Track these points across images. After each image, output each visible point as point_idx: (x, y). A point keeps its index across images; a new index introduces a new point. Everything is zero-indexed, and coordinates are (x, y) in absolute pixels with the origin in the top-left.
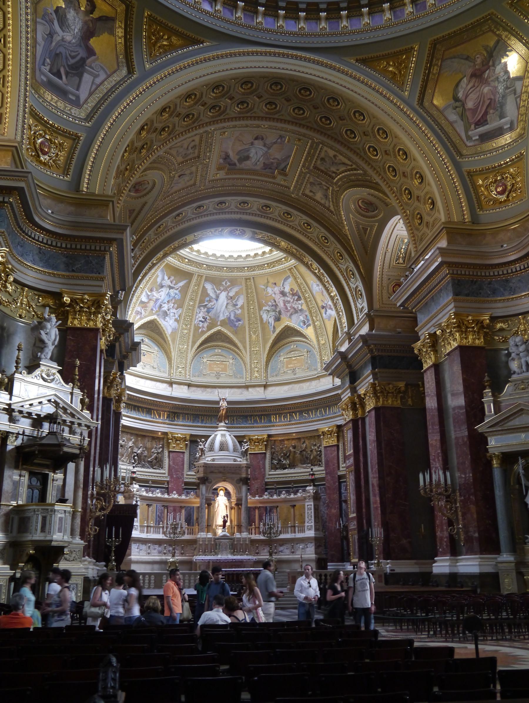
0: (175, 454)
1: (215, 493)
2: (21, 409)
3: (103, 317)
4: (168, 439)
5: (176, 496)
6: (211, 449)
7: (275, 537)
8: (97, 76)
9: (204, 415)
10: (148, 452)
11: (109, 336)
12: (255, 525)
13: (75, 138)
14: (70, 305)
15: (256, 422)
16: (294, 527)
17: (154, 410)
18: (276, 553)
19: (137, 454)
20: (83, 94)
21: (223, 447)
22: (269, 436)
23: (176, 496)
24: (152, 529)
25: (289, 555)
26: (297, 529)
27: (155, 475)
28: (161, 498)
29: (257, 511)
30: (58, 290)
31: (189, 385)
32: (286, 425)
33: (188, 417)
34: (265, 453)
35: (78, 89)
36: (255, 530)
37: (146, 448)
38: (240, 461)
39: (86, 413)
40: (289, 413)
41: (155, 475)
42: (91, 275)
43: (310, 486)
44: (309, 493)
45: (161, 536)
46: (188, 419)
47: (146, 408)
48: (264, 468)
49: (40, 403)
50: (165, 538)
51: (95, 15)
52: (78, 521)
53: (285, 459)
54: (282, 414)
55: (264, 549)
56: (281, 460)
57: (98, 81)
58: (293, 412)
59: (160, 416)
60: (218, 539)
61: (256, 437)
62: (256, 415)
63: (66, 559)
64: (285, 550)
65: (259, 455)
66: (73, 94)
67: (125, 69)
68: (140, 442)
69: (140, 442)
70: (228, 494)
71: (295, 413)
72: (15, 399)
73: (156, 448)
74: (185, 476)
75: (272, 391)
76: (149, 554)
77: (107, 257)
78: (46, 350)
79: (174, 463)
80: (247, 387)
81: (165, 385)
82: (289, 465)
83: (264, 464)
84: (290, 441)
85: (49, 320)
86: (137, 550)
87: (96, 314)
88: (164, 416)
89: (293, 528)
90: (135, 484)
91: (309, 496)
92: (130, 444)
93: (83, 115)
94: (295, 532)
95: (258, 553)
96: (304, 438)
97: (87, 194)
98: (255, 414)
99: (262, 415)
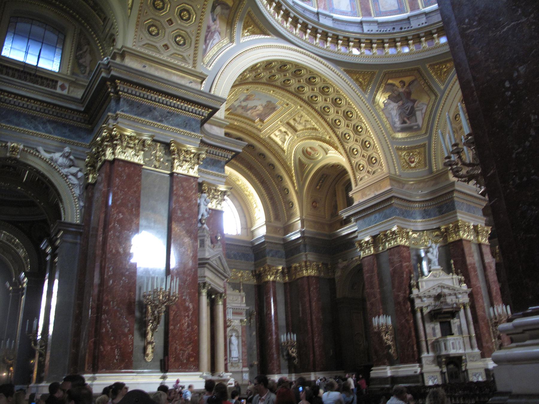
2: (424, 295)
3: (465, 231)
8: (422, 110)
11: (487, 231)
13: (424, 145)
14: (446, 232)
20: (420, 122)
30: (437, 226)
35: (416, 121)
39: (464, 285)
42: (450, 212)
49: (434, 289)
51: (407, 85)
52: (474, 341)
57: (424, 111)
63: (471, 361)
66: (416, 125)
67: (434, 95)
72: (421, 290)
77: (455, 199)
78: (432, 262)
85: (431, 247)
87: (458, 231)
93: (424, 132)
97: (437, 171)
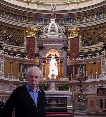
0: (30, 38)
1: (50, 58)
4: (26, 31)
5: (28, 59)
6: (46, 32)
7: (84, 81)
9: (45, 19)
10: (15, 37)
12: (72, 75)
15: (73, 21)
16: (95, 75)
17: (18, 15)
18: (84, 90)
19: (9, 38)
21: (53, 30)
22: (80, 28)
23: (28, 59)
24: (13, 76)
25: (92, 91)
26: (96, 76)
27: (18, 49)
28: (18, 59)
29: (74, 67)
31: (38, 4)
32: (89, 22)
33: (37, 19)
34: (78, 38)
36: (73, 77)
37: (14, 35)
38: (62, 37)
40: (91, 15)
41: (18, 49)
43: (104, 51)
44: (103, 54)
45: (18, 80)
46: (37, 21)
47: (13, 14)
48: (78, 46)
50: (20, 81)
53: (90, 40)
54: (87, 16)
55: (78, 88)
56: (87, 41)
58: (93, 15)
59: (21, 19)
60: (49, 81)
61: (73, 29)
62: (73, 18)
64: (90, 89)
65: (75, 39)
68: (10, 32)
69: (10, 32)
70: (56, 58)
71: (94, 15)
73: (20, 35)
74: (35, 50)
75: (81, 5)
76: (11, 90)
79: (29, 43)
80: (68, 4)
81: (25, 4)
82: (91, 43)
83: (78, 43)
84: (92, 31)
86: (2, 87)
88: (24, 19)
89: (94, 76)
90: (2, 50)
91: (103, 56)
92: (5, 32)
94: (96, 79)
95: (74, 91)
96: (99, 28)
98: (73, 17)
99: (76, 18)
